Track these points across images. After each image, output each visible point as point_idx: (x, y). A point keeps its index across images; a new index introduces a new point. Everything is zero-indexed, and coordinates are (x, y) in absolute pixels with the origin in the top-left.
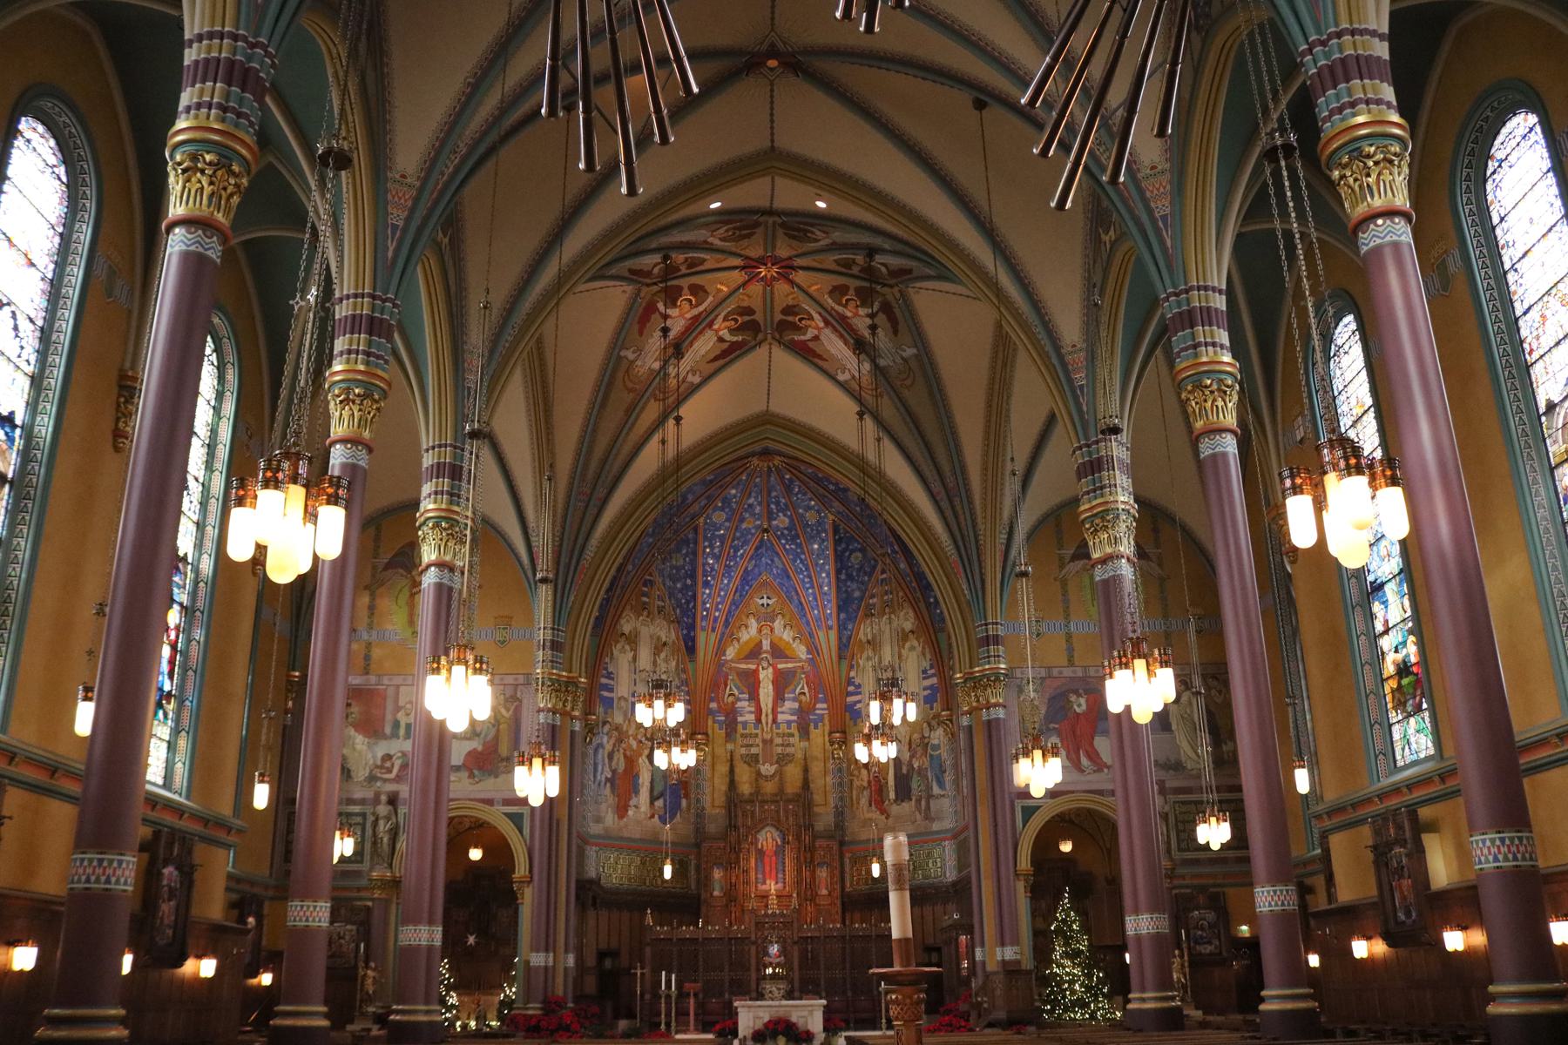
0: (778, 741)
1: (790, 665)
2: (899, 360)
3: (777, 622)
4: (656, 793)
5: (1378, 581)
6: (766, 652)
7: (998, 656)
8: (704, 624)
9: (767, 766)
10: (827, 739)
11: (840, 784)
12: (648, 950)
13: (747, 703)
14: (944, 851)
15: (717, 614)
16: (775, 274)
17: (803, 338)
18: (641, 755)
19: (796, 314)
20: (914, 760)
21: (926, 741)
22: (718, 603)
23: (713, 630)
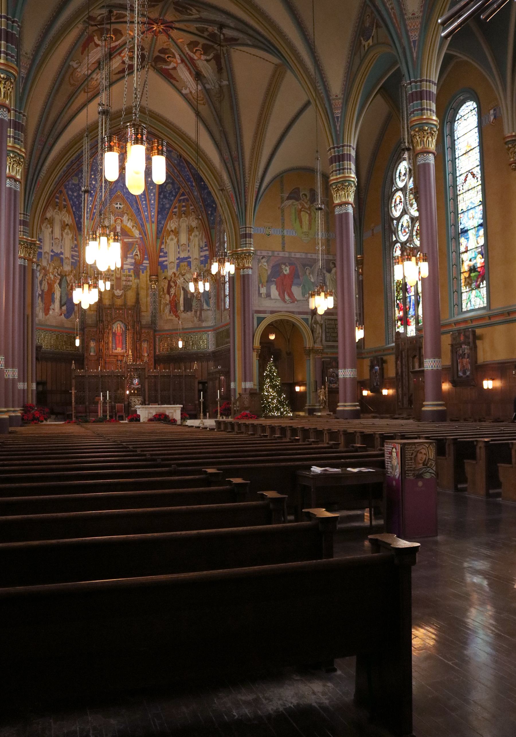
0: (124, 278)
1: (130, 240)
2: (217, 86)
3: (125, 217)
4: (63, 303)
5: (465, 229)
7: (251, 244)
9: (118, 291)
10: (148, 278)
11: (155, 302)
12: (73, 381)
14: (208, 336)
15: (95, 211)
16: (161, 30)
17: (167, 67)
18: (55, 282)
19: (165, 53)
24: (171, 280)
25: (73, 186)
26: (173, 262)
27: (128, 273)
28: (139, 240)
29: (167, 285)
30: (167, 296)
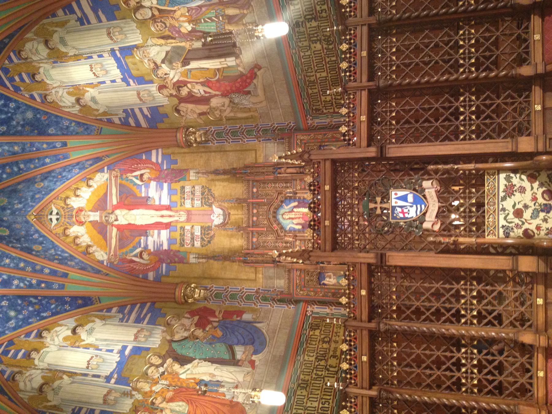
1: (114, 191)
4: (227, 357)
6: (101, 217)
8: (56, 286)
10: (186, 150)
11: (234, 133)
13: (150, 238)
15: (47, 271)
18: (177, 374)
20: (183, 30)
21: (156, 13)
22: (34, 271)
23: (65, 275)
24: (176, 96)
26: (138, 94)
28: (113, 172)
29: (190, 106)
30: (214, 102)
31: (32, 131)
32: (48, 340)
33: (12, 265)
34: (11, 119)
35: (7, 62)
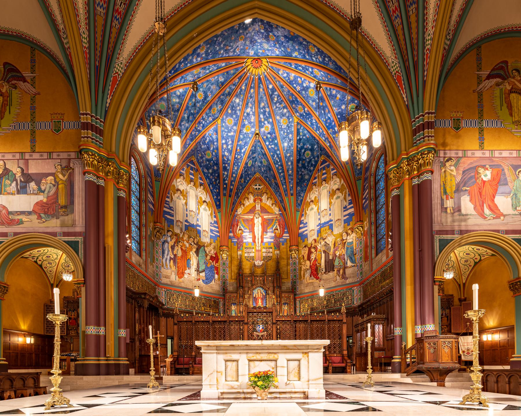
0: (264, 250)
22: (232, 181)
25: (208, 163)
27: (268, 246)
31: (298, 179)
32: (200, 190)
33: (234, 171)
34: (305, 168)
35: (332, 167)
